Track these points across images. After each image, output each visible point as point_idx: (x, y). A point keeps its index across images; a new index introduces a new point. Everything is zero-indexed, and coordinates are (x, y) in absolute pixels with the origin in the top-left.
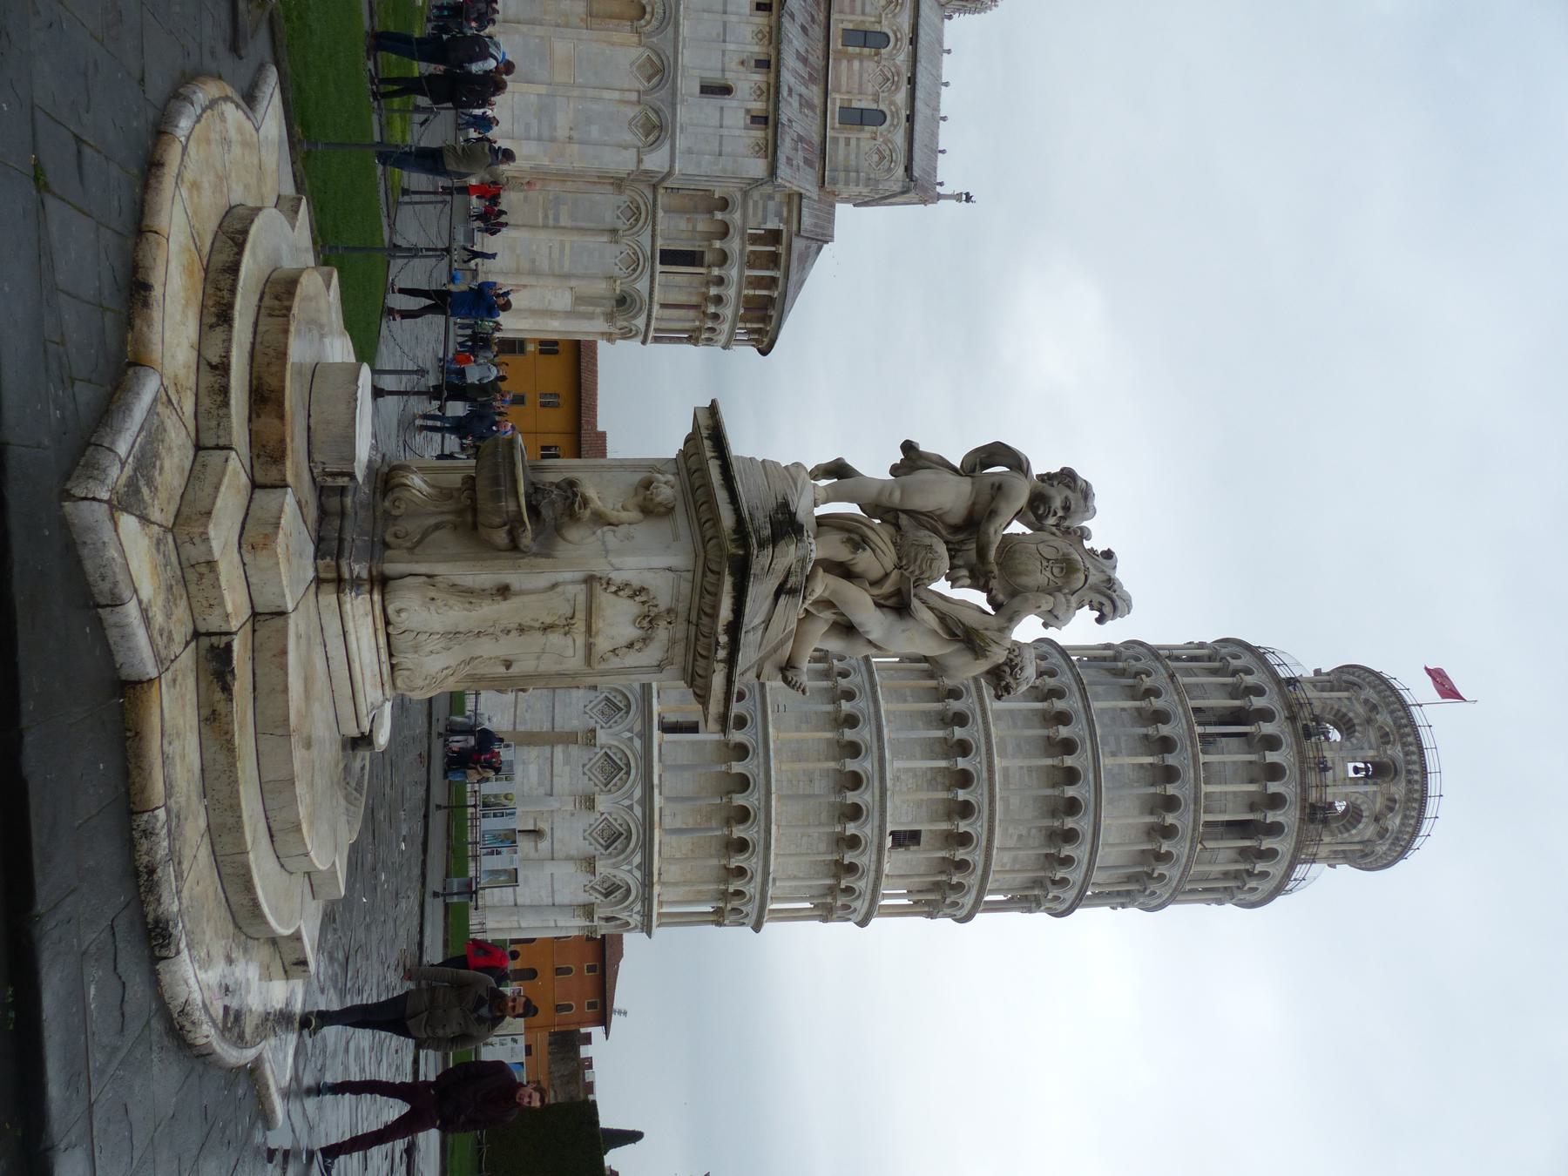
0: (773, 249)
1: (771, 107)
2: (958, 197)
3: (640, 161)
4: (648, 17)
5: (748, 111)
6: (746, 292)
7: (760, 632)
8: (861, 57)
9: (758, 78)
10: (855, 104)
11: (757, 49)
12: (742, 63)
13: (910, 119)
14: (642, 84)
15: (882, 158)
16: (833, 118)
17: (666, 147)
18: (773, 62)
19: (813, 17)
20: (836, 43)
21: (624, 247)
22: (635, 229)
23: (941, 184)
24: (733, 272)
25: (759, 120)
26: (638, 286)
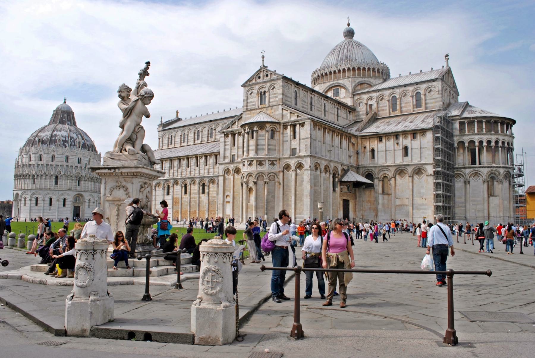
0: (466, 124)
1: (410, 133)
2: (447, 60)
3: (431, 175)
4: (387, 175)
5: (411, 140)
6: (484, 132)
7: (122, 161)
8: (401, 104)
9: (401, 138)
10: (415, 103)
11: (392, 140)
12: (398, 144)
13: (417, 84)
14: (407, 177)
15: (431, 91)
16: (420, 110)
17: (426, 166)
18: (395, 134)
19: (388, 122)
20: (397, 113)
21: (471, 179)
22: (463, 174)
23: (443, 67)
24: (476, 139)
25: (414, 137)
26: (486, 172)
